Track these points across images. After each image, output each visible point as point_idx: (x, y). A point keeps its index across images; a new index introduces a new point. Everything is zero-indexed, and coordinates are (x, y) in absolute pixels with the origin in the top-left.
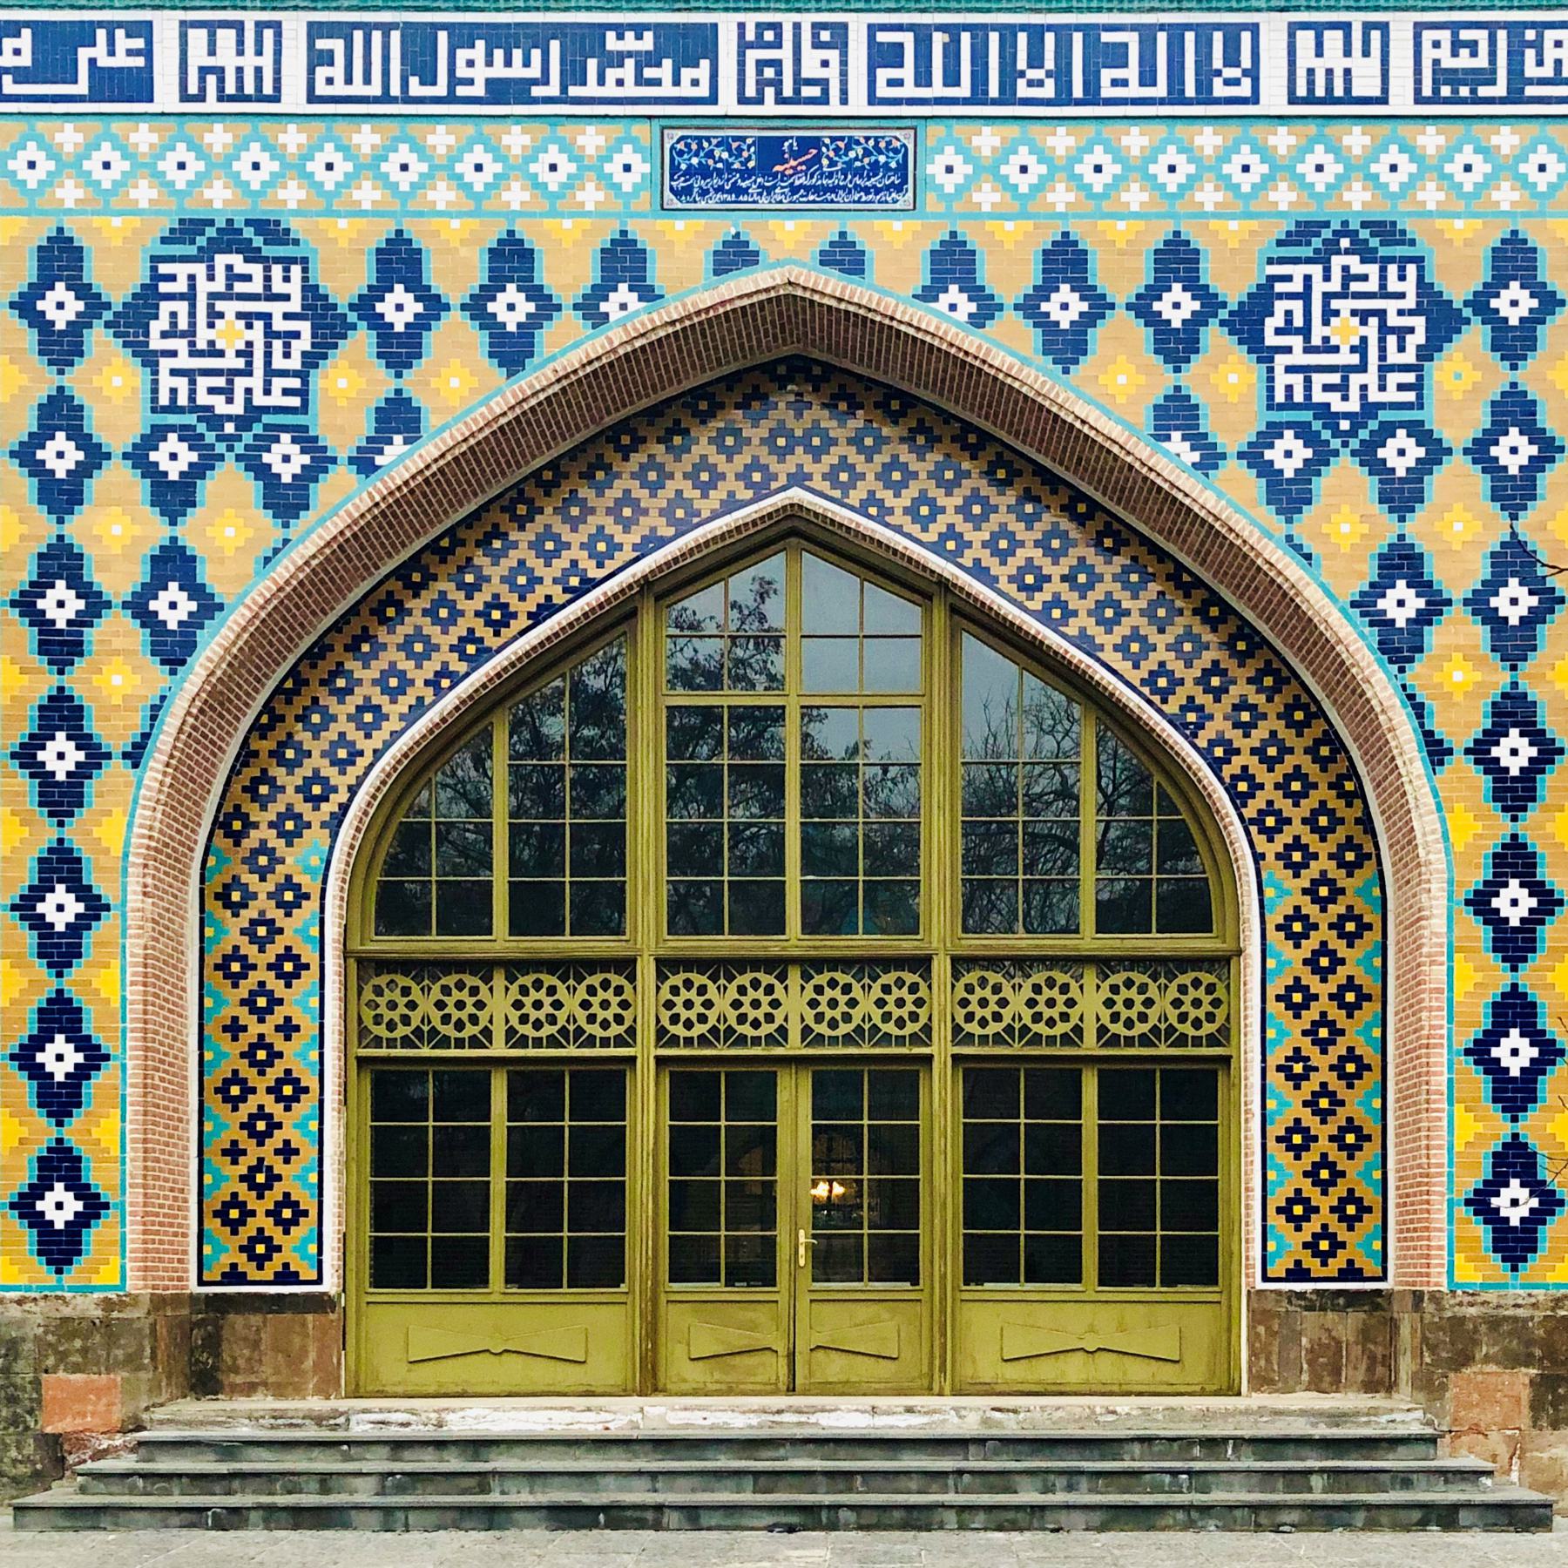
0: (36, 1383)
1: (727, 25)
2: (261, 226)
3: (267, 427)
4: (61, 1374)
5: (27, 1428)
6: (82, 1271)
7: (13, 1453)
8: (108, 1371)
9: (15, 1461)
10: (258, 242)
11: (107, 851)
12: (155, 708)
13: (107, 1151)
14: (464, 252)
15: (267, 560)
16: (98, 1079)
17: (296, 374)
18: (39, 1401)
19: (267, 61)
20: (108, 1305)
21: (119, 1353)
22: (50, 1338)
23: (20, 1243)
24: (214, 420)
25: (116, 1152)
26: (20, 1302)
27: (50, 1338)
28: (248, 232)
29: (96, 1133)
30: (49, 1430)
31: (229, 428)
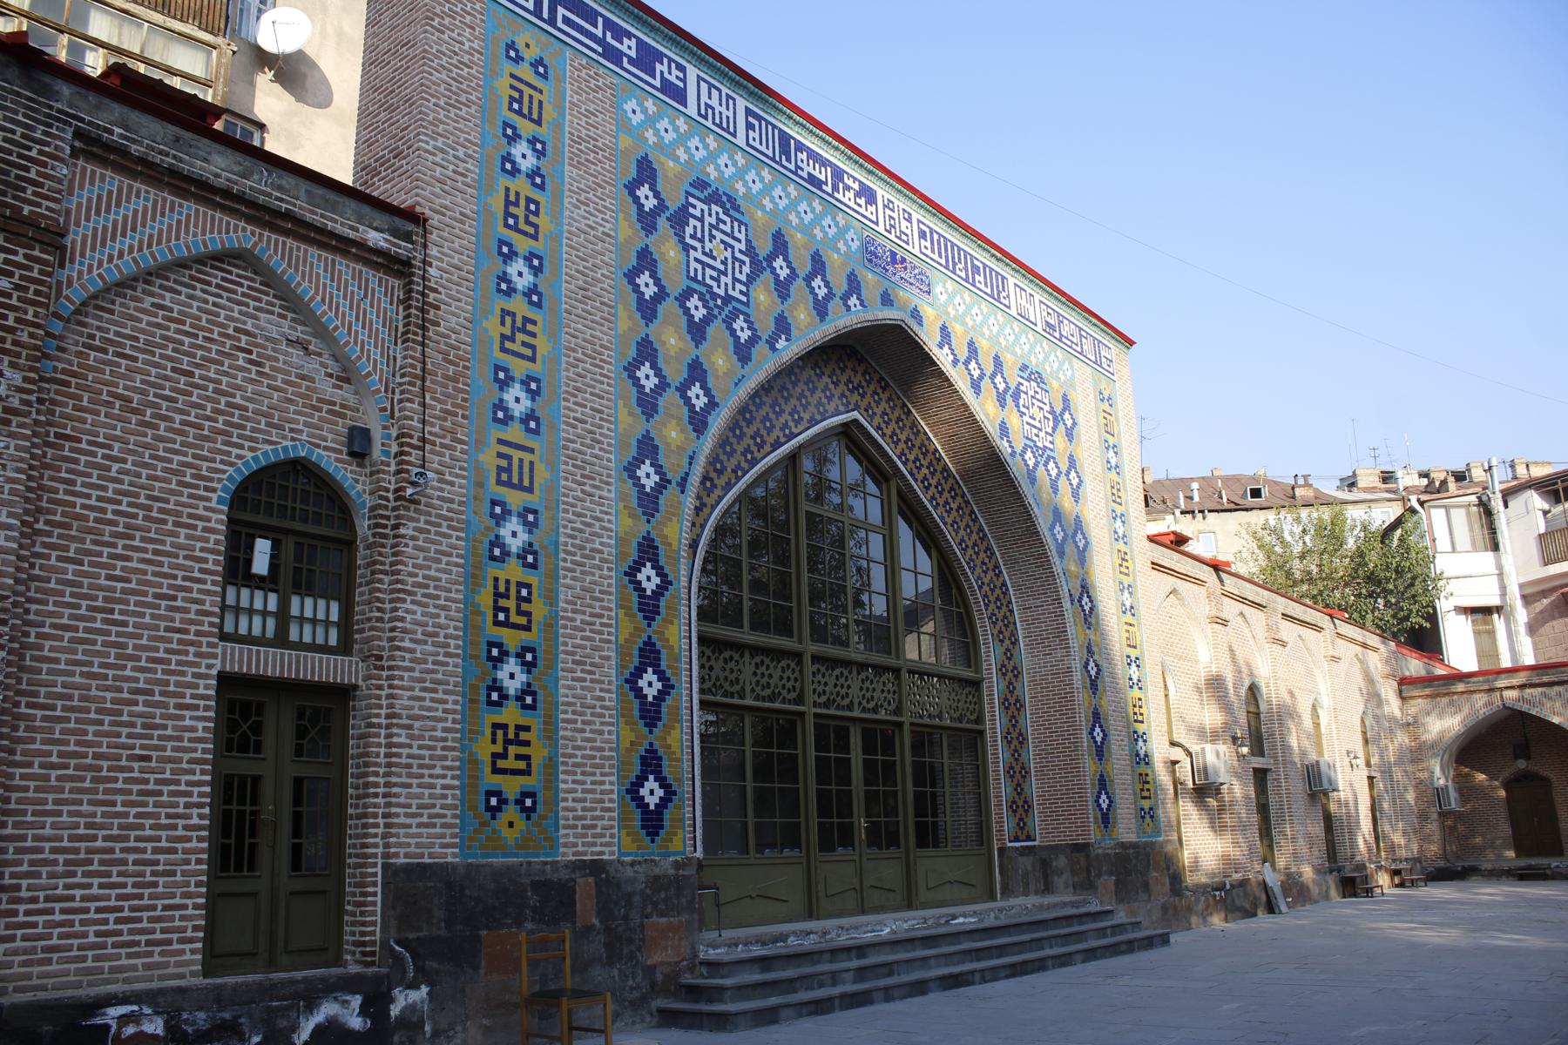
0: (642, 925)
1: (882, 193)
2: (730, 198)
3: (734, 308)
4: (655, 919)
5: (638, 962)
6: (664, 840)
7: (630, 983)
8: (679, 914)
9: (632, 988)
10: (728, 205)
11: (670, 545)
12: (691, 458)
13: (674, 753)
14: (802, 251)
15: (736, 384)
16: (669, 700)
17: (744, 284)
18: (643, 940)
19: (731, 114)
20: (676, 865)
21: (684, 900)
22: (648, 891)
23: (633, 820)
24: (714, 296)
25: (678, 751)
26: (633, 864)
27: (648, 891)
28: (724, 199)
29: (669, 741)
30: (649, 962)
31: (719, 302)
